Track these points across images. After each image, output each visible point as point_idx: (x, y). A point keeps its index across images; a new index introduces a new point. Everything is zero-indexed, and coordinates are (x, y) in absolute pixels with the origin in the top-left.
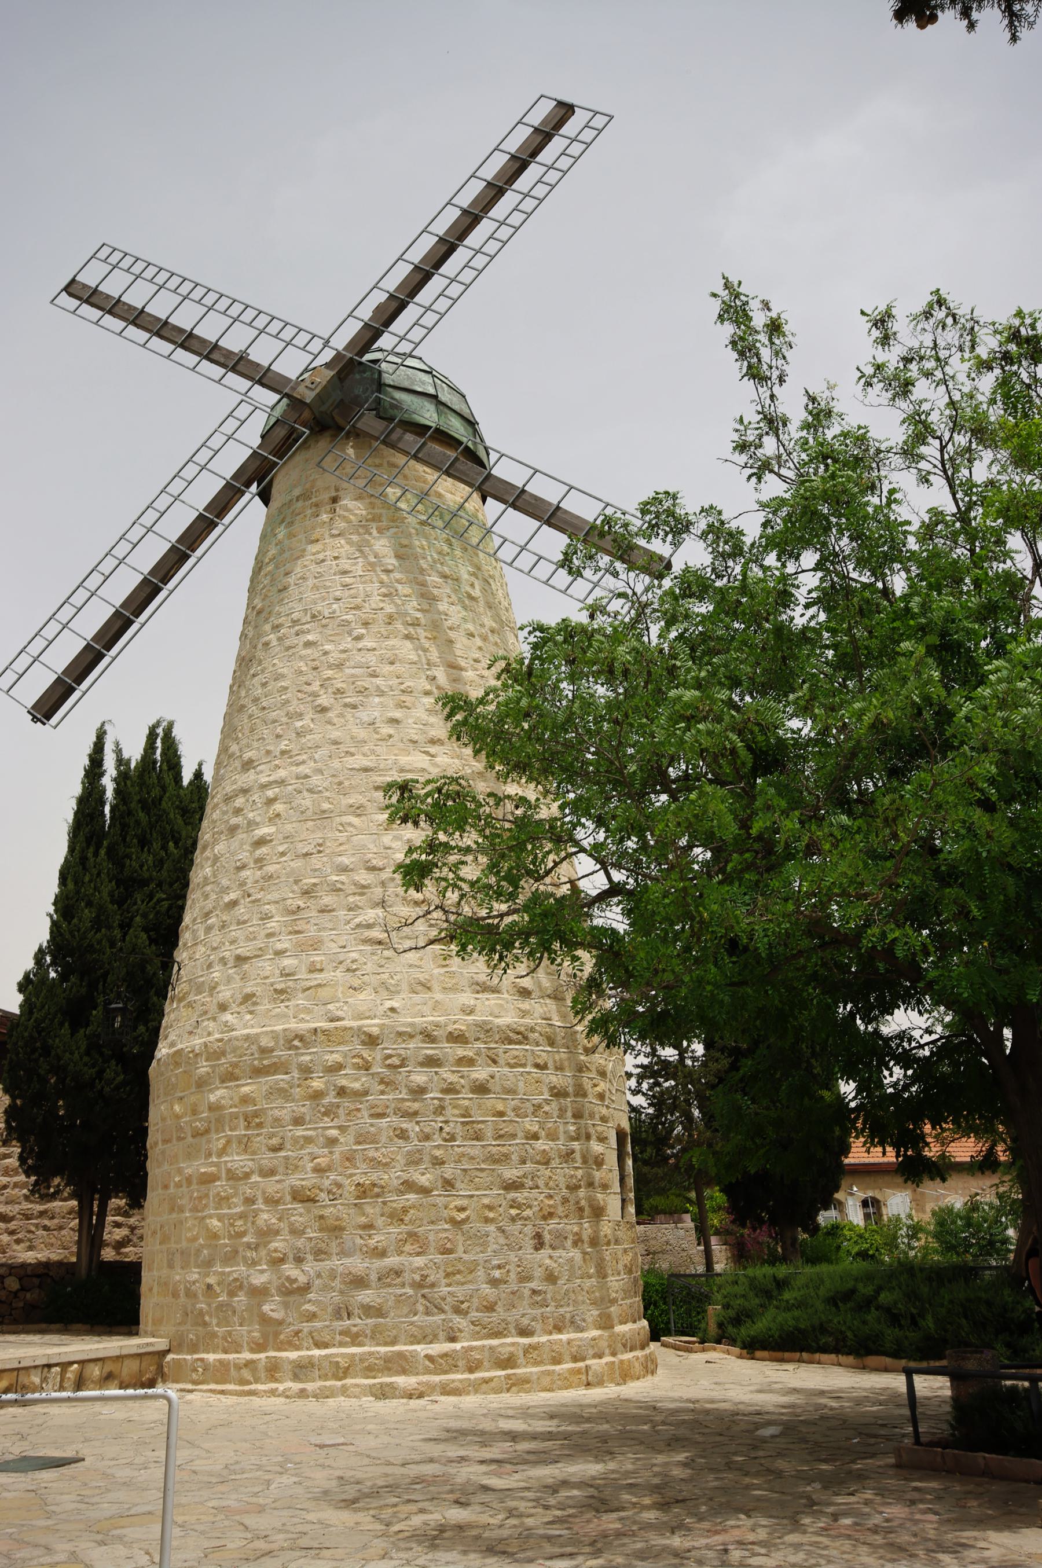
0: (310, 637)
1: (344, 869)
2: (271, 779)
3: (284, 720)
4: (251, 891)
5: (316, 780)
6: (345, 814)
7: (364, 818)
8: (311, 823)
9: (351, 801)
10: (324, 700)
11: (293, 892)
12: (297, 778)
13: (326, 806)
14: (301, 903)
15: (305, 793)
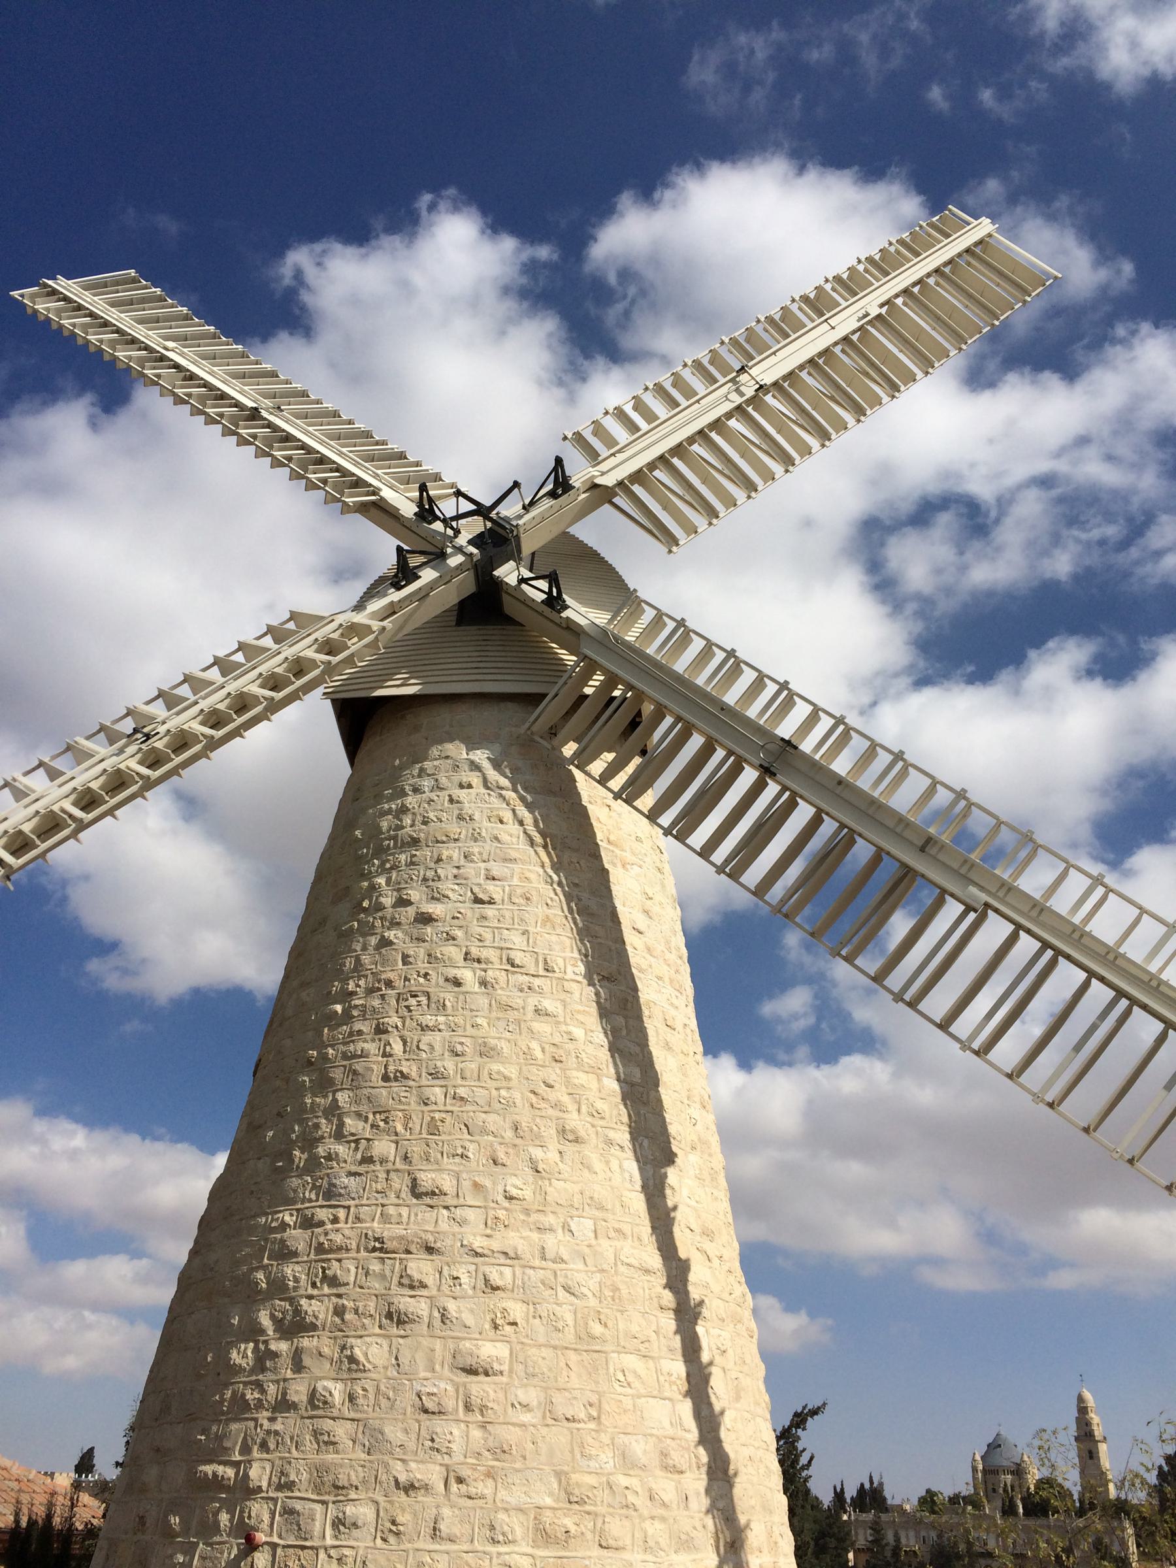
0: (548, 1004)
1: (628, 1462)
2: (496, 1245)
3: (509, 1134)
4: (465, 1472)
5: (576, 1272)
6: (624, 1350)
7: (651, 1363)
8: (573, 1357)
9: (635, 1328)
10: (574, 1120)
11: (551, 1494)
12: (544, 1258)
13: (597, 1329)
14: (569, 1523)
15: (561, 1293)
